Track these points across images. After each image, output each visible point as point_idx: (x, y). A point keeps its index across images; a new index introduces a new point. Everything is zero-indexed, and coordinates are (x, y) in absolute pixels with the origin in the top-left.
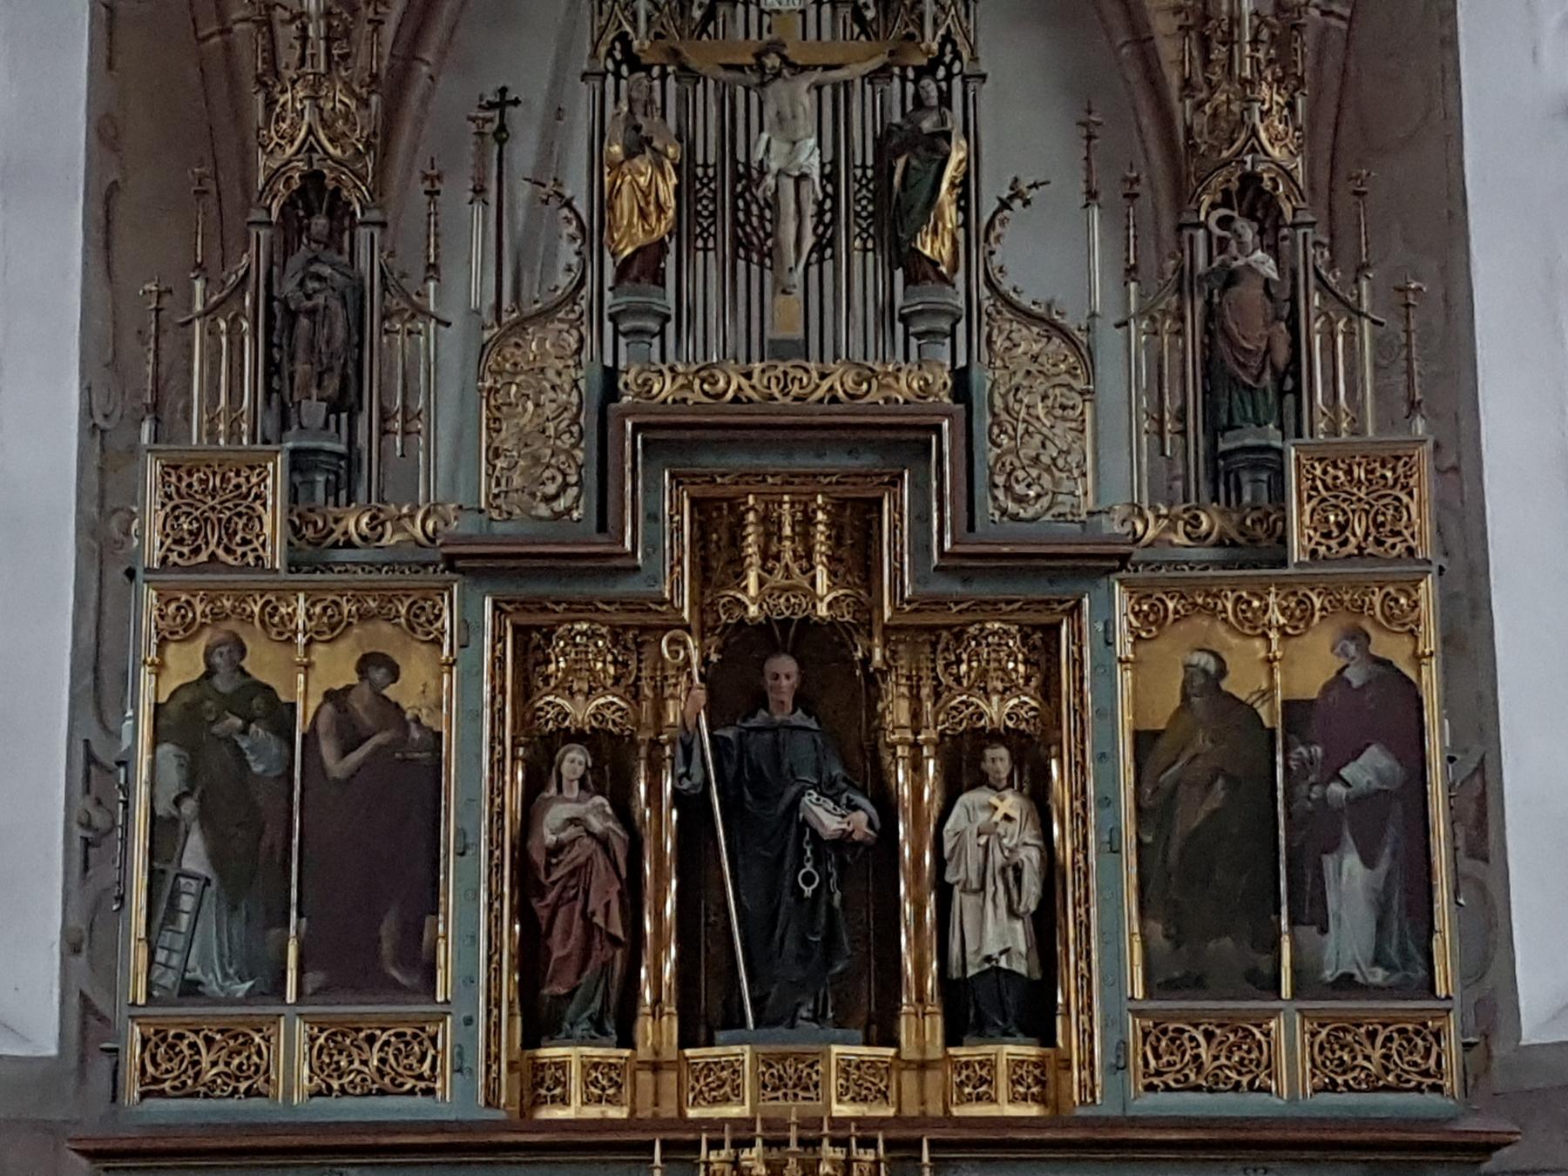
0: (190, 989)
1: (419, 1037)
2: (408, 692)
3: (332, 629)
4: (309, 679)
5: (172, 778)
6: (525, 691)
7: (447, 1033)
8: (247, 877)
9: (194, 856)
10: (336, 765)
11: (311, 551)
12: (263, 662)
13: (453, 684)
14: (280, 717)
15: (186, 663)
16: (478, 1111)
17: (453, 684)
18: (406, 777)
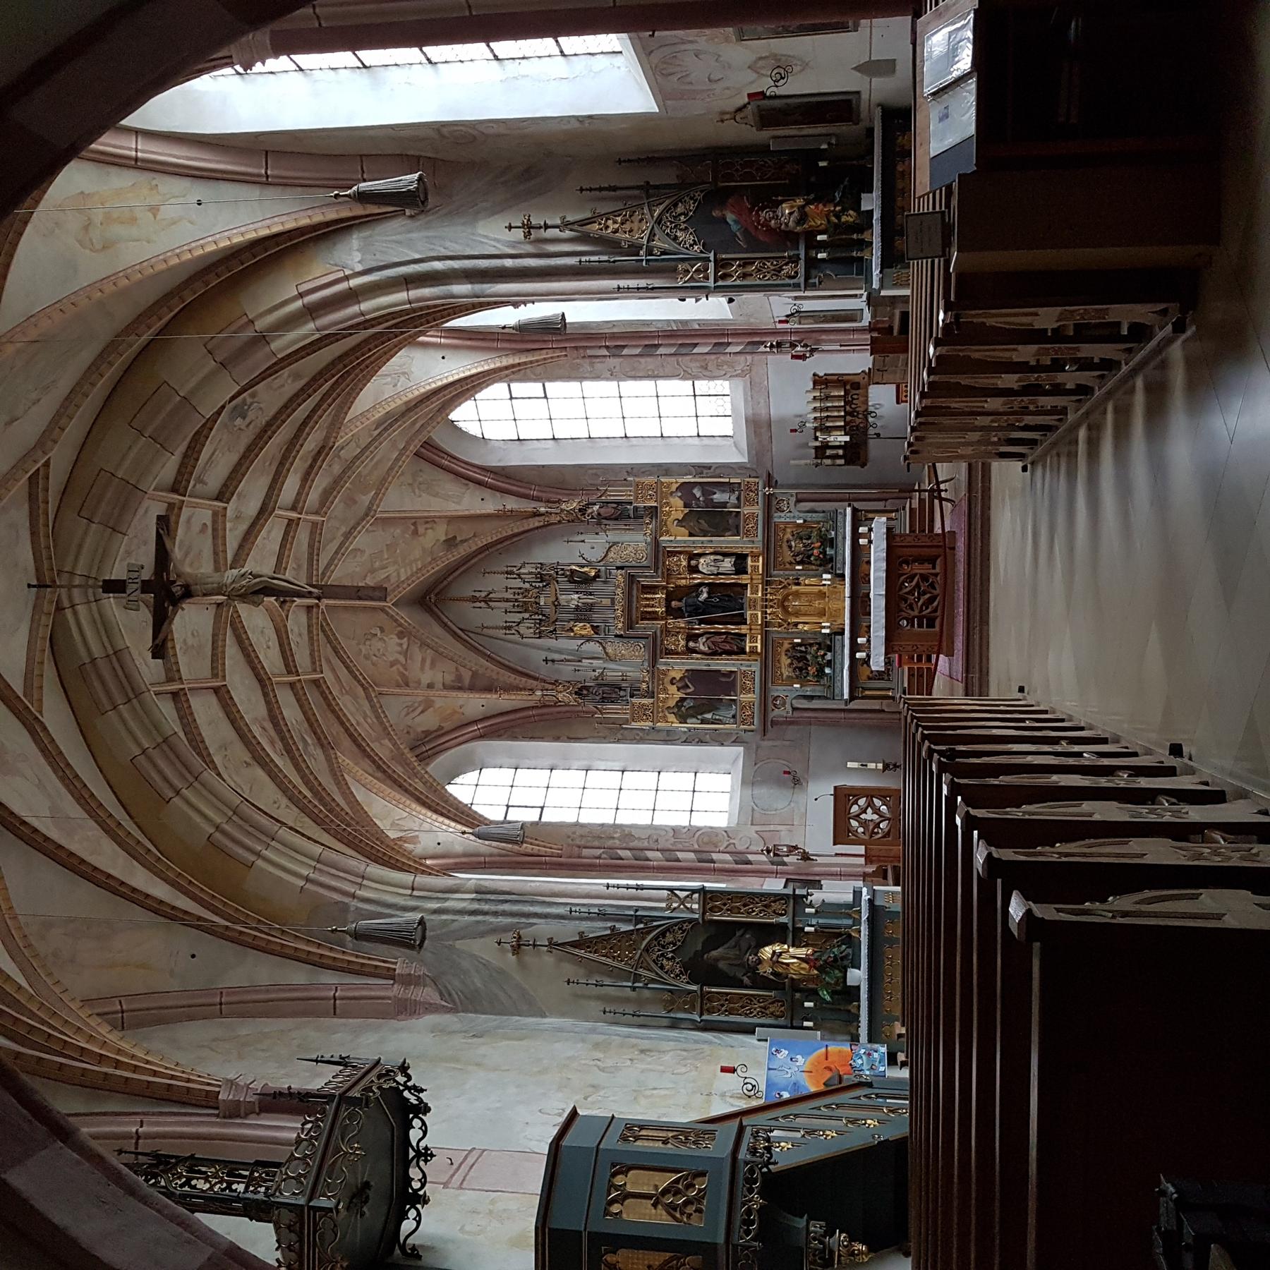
0: (734, 717)
1: (744, 674)
2: (678, 676)
3: (665, 690)
4: (675, 694)
5: (694, 720)
6: (677, 653)
7: (743, 668)
8: (712, 706)
9: (709, 716)
10: (692, 689)
11: (650, 694)
12: (672, 703)
13: (677, 667)
14: (682, 700)
15: (672, 718)
16: (758, 663)
17: (677, 667)
18: (694, 675)
